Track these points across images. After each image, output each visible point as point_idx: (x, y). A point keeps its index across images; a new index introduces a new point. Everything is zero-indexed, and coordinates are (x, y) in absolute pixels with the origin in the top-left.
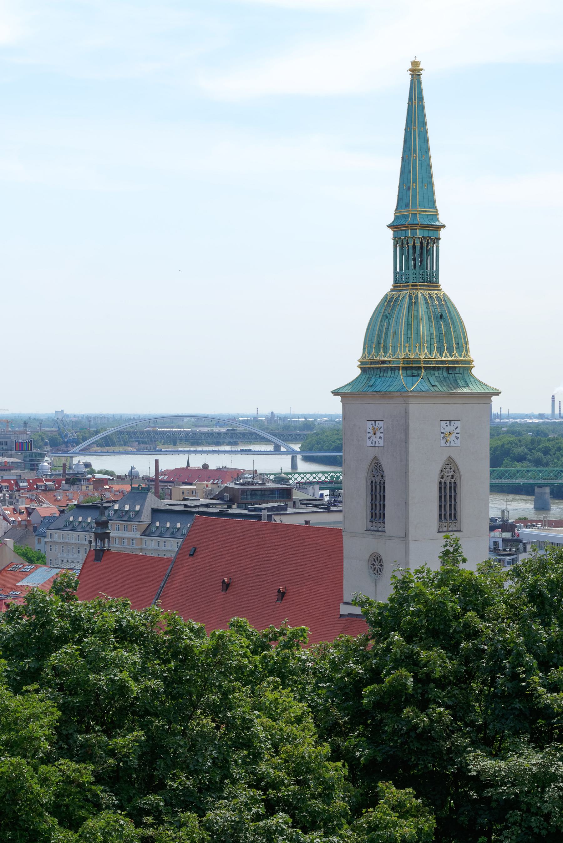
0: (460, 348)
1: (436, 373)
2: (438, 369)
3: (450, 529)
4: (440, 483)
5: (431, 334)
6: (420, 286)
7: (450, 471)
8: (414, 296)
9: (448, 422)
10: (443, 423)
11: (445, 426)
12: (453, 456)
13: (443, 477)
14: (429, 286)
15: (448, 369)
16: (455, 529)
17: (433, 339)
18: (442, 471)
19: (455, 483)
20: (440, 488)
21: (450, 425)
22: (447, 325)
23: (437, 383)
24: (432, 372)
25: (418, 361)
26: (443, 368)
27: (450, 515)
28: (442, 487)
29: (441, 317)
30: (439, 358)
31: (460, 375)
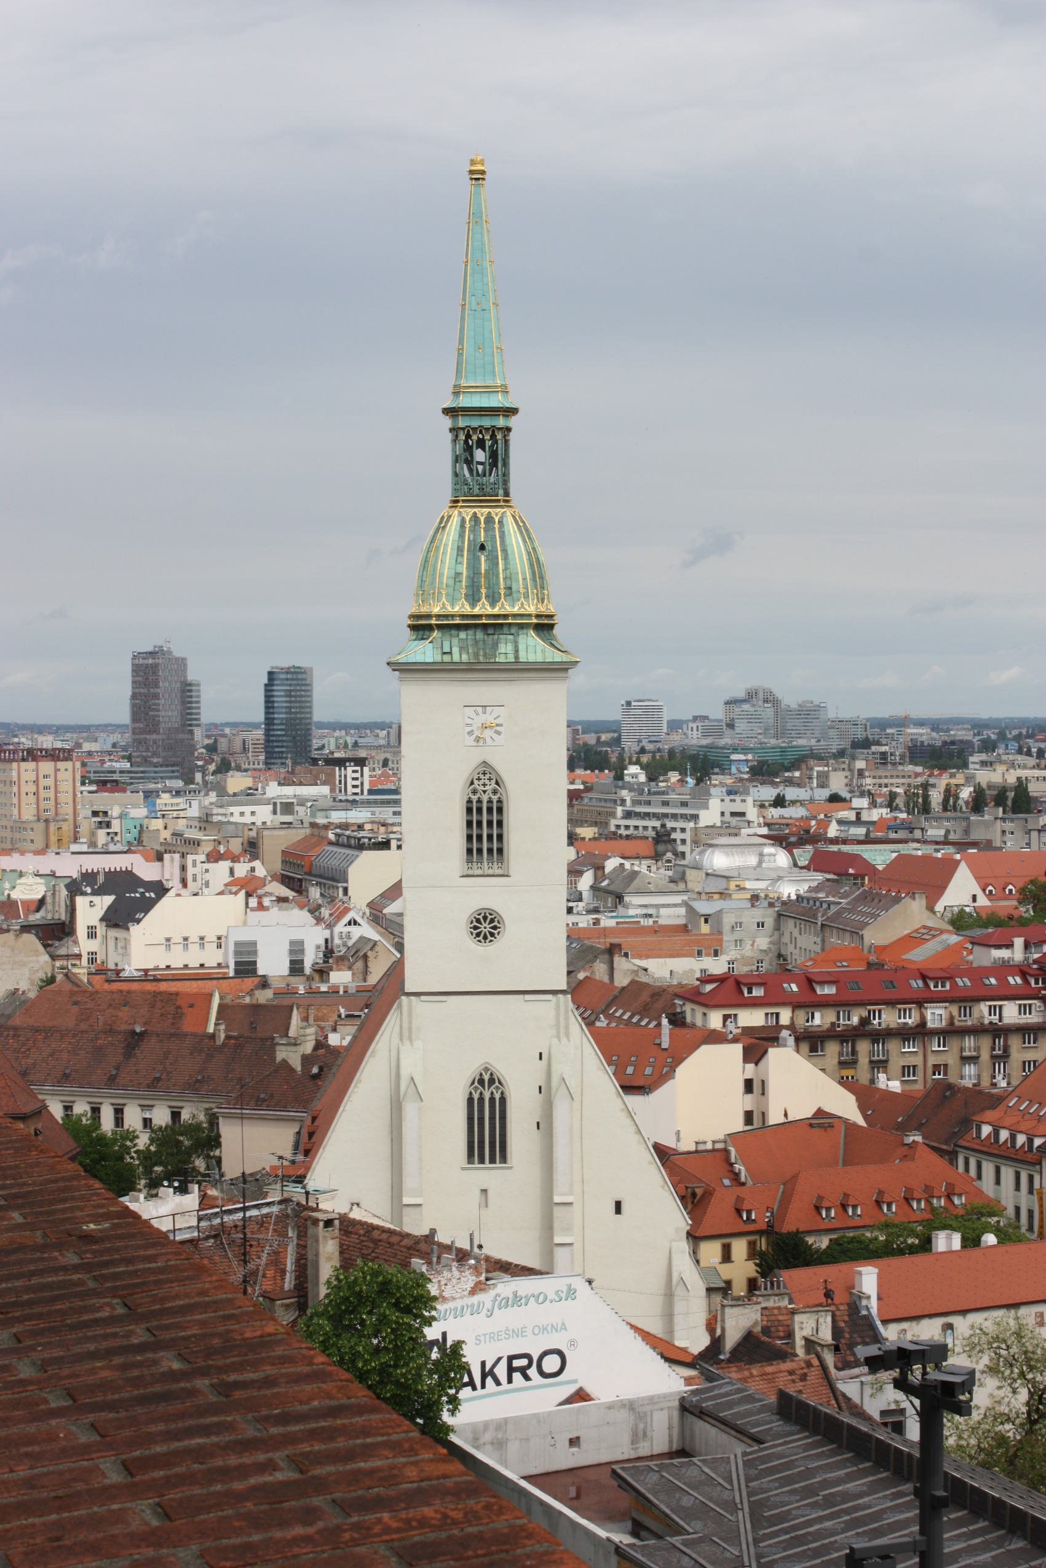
0: (515, 595)
1: (463, 635)
2: (466, 627)
3: (491, 872)
4: (470, 801)
5: (458, 575)
6: (464, 501)
7: (487, 782)
8: (468, 519)
9: (480, 709)
10: (469, 711)
11: (473, 715)
12: (490, 761)
13: (474, 792)
14: (481, 501)
15: (485, 626)
16: (500, 872)
17: (460, 581)
18: (472, 783)
19: (500, 801)
20: (469, 810)
21: (485, 713)
22: (493, 561)
23: (456, 650)
24: (454, 632)
25: (429, 616)
26: (476, 626)
27: (490, 851)
29: (482, 547)
30: (467, 610)
31: (511, 637)
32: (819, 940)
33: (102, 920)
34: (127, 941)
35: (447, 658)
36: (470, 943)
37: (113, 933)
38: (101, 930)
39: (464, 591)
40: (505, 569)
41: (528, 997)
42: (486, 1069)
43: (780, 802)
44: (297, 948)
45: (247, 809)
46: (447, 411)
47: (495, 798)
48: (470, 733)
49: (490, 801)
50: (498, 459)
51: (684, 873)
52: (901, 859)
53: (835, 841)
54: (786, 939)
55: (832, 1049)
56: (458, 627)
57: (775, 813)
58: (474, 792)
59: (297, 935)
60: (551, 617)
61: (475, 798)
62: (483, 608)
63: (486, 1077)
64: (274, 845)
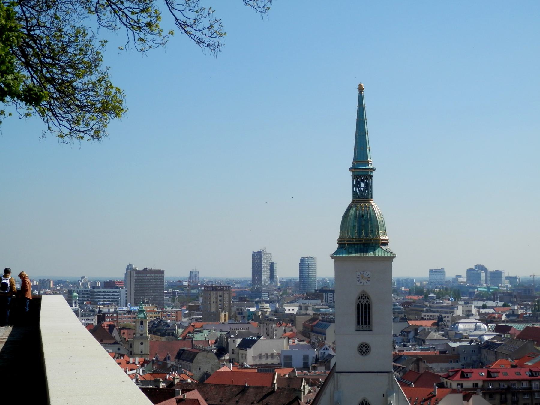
1: (356, 247)
2: (357, 244)
4: (358, 305)
9: (362, 272)
10: (358, 273)
11: (360, 274)
13: (360, 302)
19: (369, 305)
22: (367, 221)
23: (353, 252)
24: (353, 246)
28: (359, 308)
29: (363, 216)
32: (494, 357)
33: (238, 347)
34: (246, 355)
35: (350, 255)
36: (358, 355)
37: (241, 352)
38: (237, 350)
39: (356, 232)
40: (371, 223)
41: (379, 374)
42: (364, 400)
43: (484, 307)
44: (306, 358)
45: (291, 308)
46: (351, 169)
47: (367, 304)
48: (359, 281)
49: (366, 305)
50: (368, 186)
51: (448, 333)
52: (527, 328)
53: (504, 322)
54: (483, 357)
55: (498, 397)
56: (354, 244)
57: (483, 311)
58: (360, 302)
59: (306, 354)
60: (387, 240)
61: (360, 304)
62: (363, 237)
63: (364, 403)
64: (301, 320)
